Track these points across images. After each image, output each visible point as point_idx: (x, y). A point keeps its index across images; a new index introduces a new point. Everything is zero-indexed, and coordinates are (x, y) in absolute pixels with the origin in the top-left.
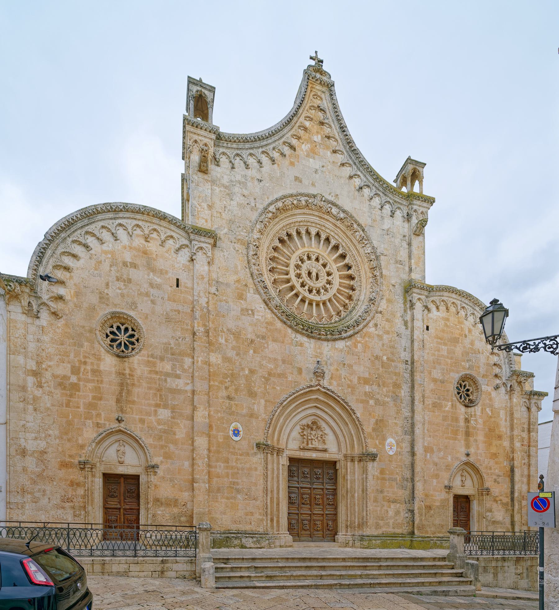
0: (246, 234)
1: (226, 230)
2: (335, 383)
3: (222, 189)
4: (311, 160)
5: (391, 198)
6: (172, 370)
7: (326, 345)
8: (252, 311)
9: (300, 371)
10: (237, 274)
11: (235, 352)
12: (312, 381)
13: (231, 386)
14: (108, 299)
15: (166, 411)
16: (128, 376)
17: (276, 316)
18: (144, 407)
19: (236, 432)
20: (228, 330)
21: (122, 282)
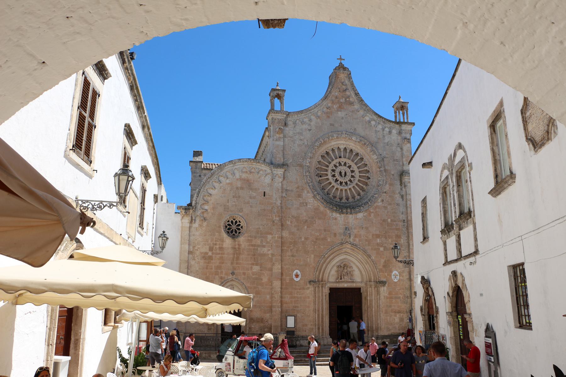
0: (302, 161)
1: (291, 161)
2: (357, 240)
3: (289, 138)
4: (339, 113)
5: (388, 125)
6: (261, 243)
7: (351, 217)
8: (306, 203)
9: (335, 235)
10: (297, 184)
12: (342, 240)
14: (228, 208)
15: (257, 266)
16: (237, 249)
18: (245, 266)
19: (297, 276)
20: (292, 216)
21: (235, 198)
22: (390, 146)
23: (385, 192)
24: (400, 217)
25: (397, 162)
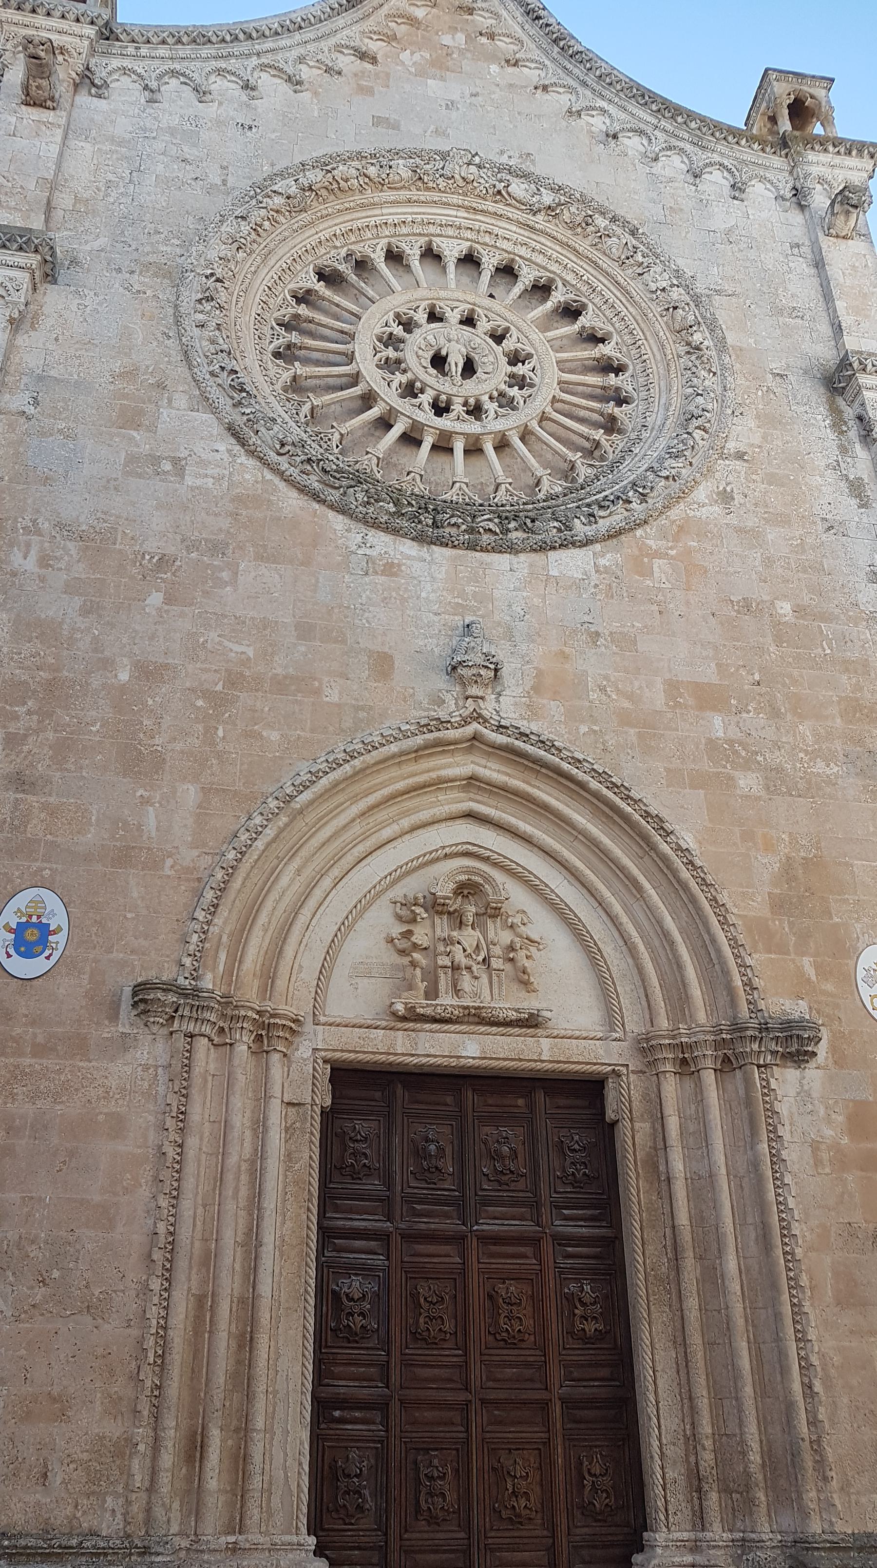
11: (78, 601)
13: (37, 732)
17: (281, 474)
22: (743, 246)
23: (740, 456)
24: (862, 598)
25: (799, 321)
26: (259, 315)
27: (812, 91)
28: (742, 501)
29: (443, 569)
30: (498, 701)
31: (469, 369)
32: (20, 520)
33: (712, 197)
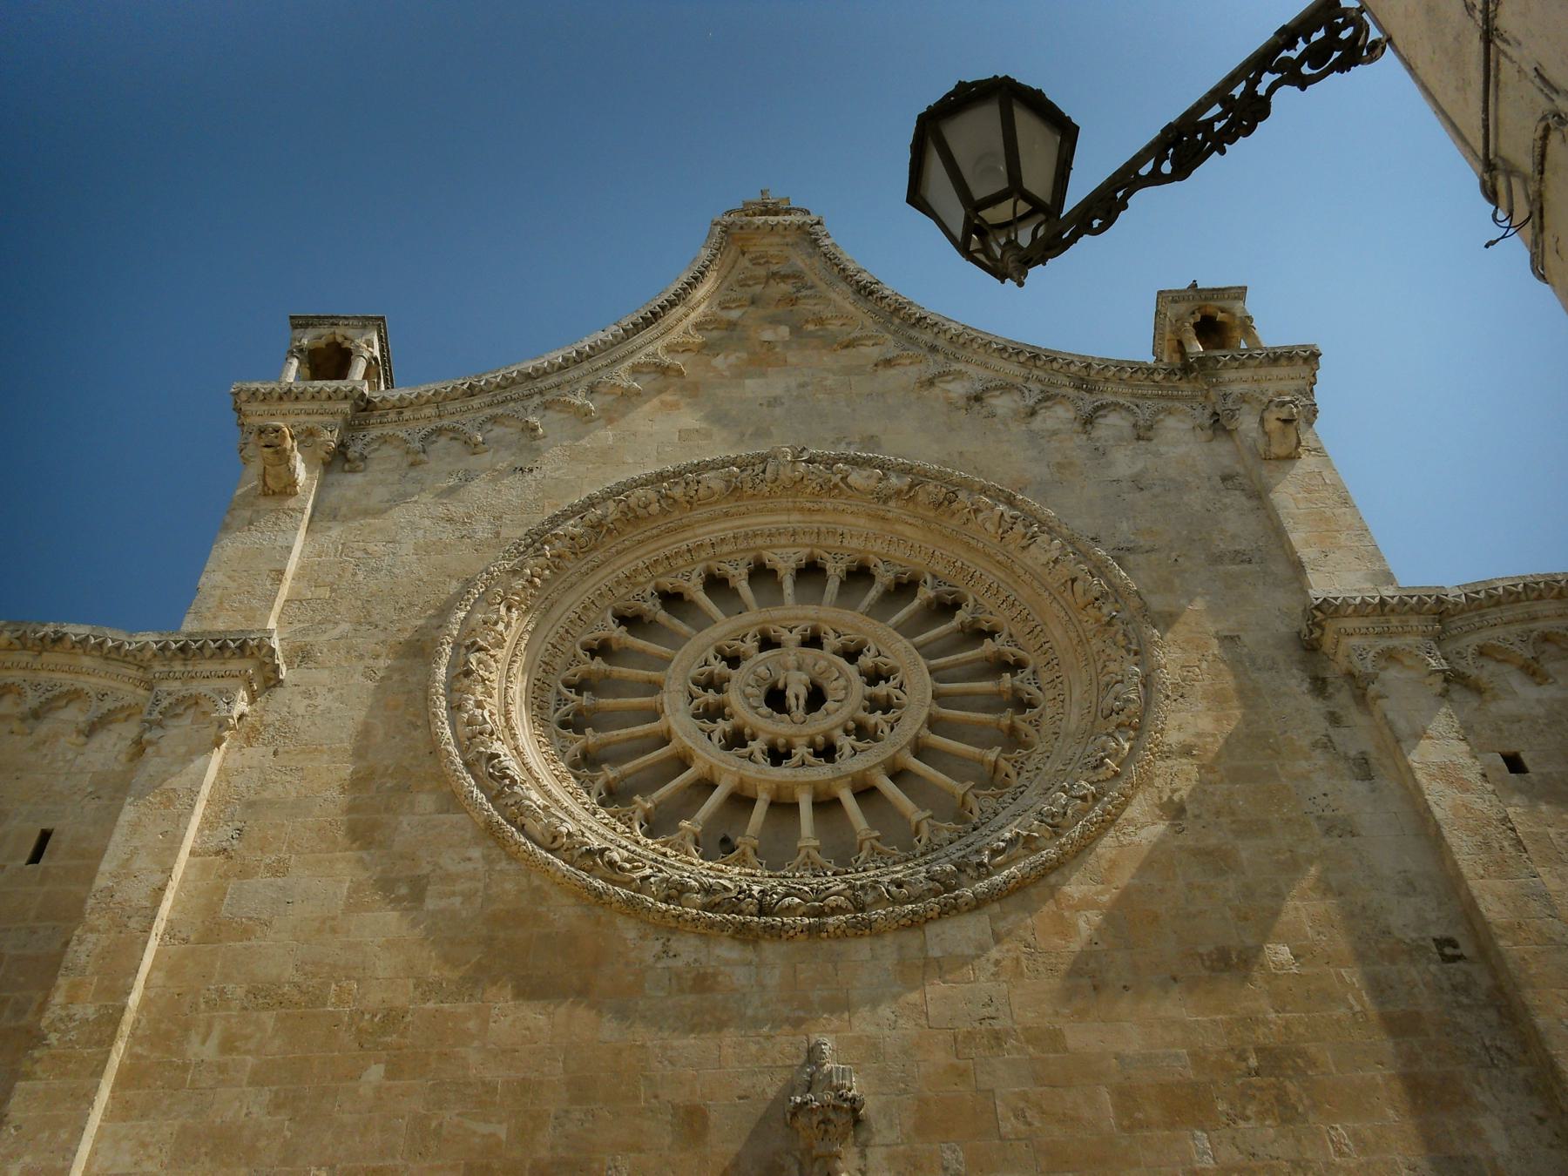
11: (266, 1095)
25: (1246, 566)
26: (539, 680)
27: (1220, 304)
28: (1197, 812)
29: (777, 972)
30: (863, 1156)
31: (816, 698)
32: (203, 992)
33: (1111, 442)
